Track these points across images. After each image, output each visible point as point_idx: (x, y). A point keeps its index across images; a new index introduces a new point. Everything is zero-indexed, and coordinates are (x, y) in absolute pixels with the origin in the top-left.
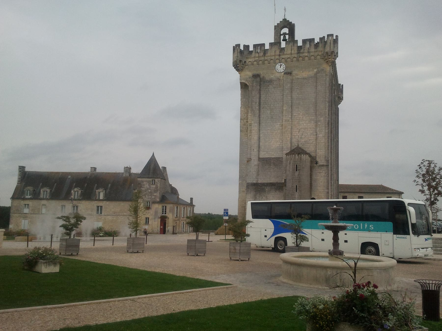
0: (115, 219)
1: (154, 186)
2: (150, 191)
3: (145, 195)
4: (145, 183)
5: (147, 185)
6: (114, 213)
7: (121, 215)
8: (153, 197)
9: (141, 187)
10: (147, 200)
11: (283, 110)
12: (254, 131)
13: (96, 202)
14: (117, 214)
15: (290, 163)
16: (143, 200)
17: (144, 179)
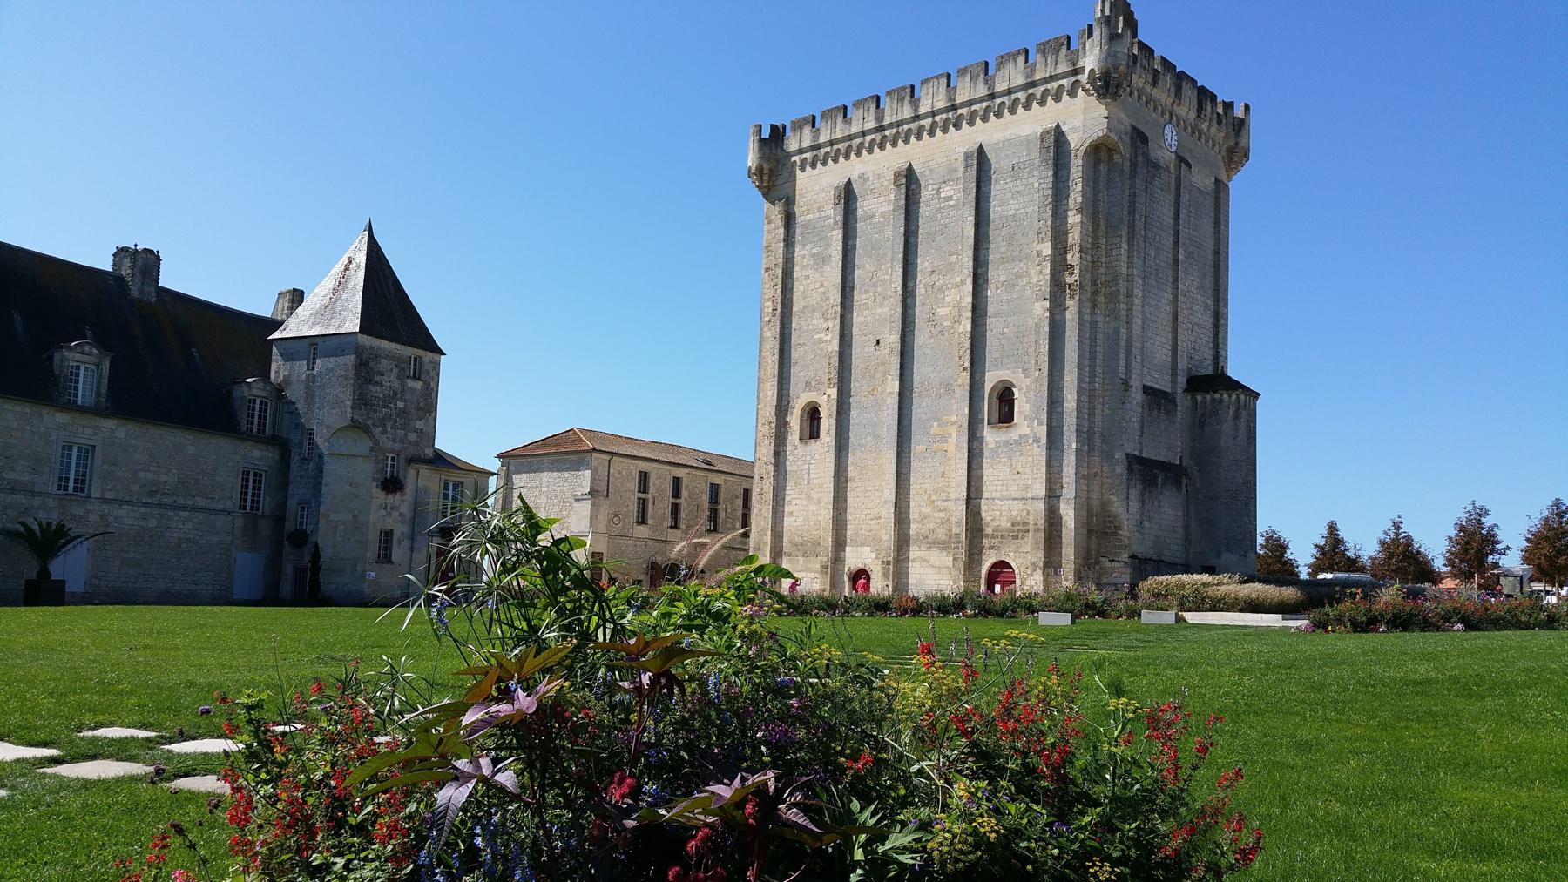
0: (152, 523)
1: (418, 385)
2: (401, 405)
3: (383, 422)
4: (384, 364)
5: (393, 378)
6: (152, 494)
7: (184, 508)
8: (412, 436)
9: (371, 382)
10: (389, 444)
11: (1176, 261)
12: (1137, 301)
13: (61, 417)
14: (166, 500)
15: (1237, 417)
16: (376, 442)
17: (385, 344)
